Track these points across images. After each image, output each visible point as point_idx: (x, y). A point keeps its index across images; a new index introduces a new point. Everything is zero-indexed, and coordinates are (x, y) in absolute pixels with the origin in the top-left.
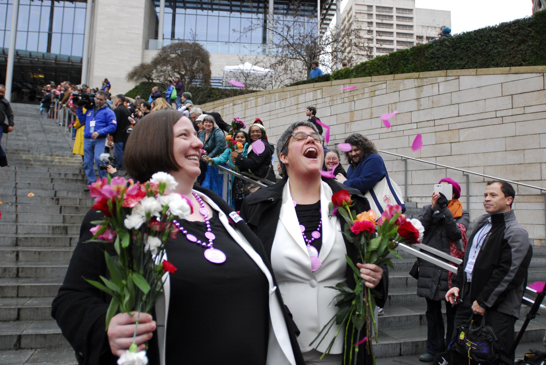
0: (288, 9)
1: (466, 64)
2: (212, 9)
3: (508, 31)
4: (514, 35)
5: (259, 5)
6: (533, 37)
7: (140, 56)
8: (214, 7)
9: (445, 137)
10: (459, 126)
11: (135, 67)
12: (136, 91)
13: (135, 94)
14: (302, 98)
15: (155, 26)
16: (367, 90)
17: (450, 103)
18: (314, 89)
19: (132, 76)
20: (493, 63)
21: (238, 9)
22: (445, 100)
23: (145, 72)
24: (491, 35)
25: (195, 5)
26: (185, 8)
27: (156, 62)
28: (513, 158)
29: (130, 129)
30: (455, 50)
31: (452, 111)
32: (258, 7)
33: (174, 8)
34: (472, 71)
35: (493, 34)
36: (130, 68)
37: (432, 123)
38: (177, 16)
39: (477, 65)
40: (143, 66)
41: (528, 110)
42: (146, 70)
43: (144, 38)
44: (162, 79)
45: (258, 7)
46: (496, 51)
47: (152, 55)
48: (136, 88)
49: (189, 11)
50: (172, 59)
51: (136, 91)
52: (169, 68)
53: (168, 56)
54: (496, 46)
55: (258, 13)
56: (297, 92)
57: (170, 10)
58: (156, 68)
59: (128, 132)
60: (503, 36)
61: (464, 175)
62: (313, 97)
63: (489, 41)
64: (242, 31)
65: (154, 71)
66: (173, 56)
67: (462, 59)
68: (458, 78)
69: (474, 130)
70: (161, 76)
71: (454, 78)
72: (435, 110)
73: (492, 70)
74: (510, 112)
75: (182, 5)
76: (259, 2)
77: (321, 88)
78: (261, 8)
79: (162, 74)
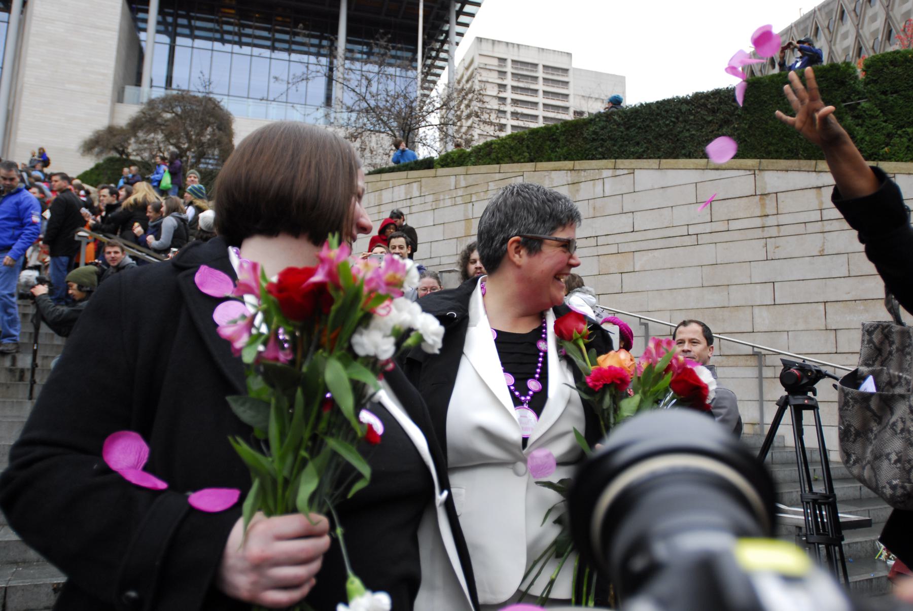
0: (370, 54)
1: (644, 151)
2: (241, 44)
3: (705, 105)
4: (713, 112)
5: (320, 42)
6: (739, 116)
7: (107, 114)
8: (244, 40)
9: (613, 263)
10: (634, 247)
11: (97, 132)
12: (97, 172)
13: (94, 177)
14: (387, 196)
15: (136, 63)
16: (492, 186)
17: (620, 211)
18: (408, 181)
19: (90, 146)
20: (683, 152)
21: (286, 46)
22: (612, 206)
23: (114, 140)
24: (680, 110)
25: (210, 34)
26: (193, 37)
27: (136, 125)
28: (713, 298)
29: (81, 233)
30: (628, 129)
31: (624, 223)
32: (320, 46)
33: (173, 36)
34: (654, 163)
35: (684, 108)
36: (87, 133)
37: (593, 242)
38: (177, 49)
39: (661, 154)
40: (111, 131)
41: (734, 225)
42: (117, 137)
43: (115, 82)
44: (146, 155)
45: (320, 46)
46: (687, 134)
47: (128, 113)
48: (98, 167)
49: (198, 43)
50: (167, 121)
51: (97, 172)
52: (160, 137)
53: (159, 115)
54: (688, 127)
55: (318, 55)
56: (380, 185)
57: (166, 39)
58: (135, 136)
59: (76, 238)
60: (697, 112)
61: (641, 324)
62: (406, 194)
63: (677, 118)
64: (290, 81)
65: (132, 140)
66: (168, 116)
67: (638, 144)
68: (632, 171)
69: (656, 253)
70: (145, 149)
71: (626, 172)
72: (599, 221)
73: (682, 162)
74: (708, 228)
75: (187, 31)
76: (321, 38)
77: (418, 180)
78: (323, 47)
79: (146, 145)
